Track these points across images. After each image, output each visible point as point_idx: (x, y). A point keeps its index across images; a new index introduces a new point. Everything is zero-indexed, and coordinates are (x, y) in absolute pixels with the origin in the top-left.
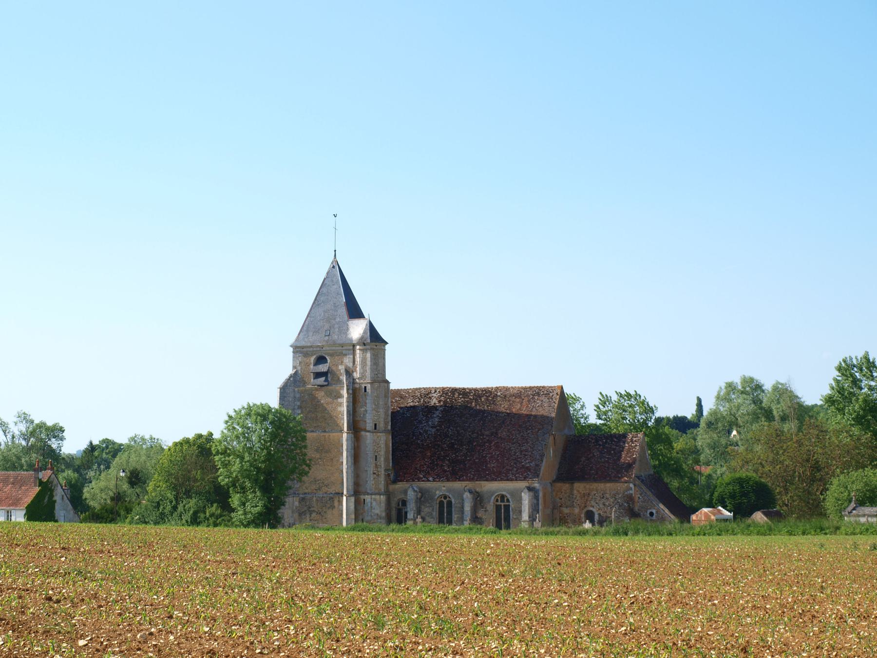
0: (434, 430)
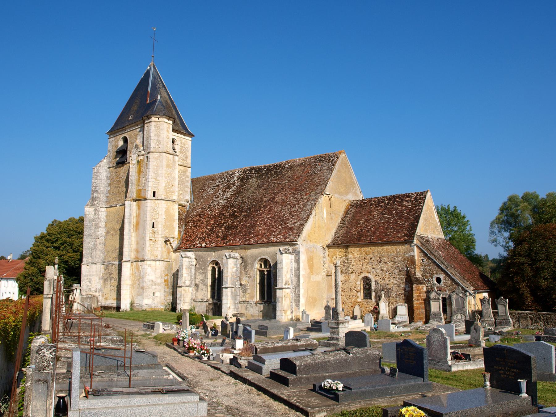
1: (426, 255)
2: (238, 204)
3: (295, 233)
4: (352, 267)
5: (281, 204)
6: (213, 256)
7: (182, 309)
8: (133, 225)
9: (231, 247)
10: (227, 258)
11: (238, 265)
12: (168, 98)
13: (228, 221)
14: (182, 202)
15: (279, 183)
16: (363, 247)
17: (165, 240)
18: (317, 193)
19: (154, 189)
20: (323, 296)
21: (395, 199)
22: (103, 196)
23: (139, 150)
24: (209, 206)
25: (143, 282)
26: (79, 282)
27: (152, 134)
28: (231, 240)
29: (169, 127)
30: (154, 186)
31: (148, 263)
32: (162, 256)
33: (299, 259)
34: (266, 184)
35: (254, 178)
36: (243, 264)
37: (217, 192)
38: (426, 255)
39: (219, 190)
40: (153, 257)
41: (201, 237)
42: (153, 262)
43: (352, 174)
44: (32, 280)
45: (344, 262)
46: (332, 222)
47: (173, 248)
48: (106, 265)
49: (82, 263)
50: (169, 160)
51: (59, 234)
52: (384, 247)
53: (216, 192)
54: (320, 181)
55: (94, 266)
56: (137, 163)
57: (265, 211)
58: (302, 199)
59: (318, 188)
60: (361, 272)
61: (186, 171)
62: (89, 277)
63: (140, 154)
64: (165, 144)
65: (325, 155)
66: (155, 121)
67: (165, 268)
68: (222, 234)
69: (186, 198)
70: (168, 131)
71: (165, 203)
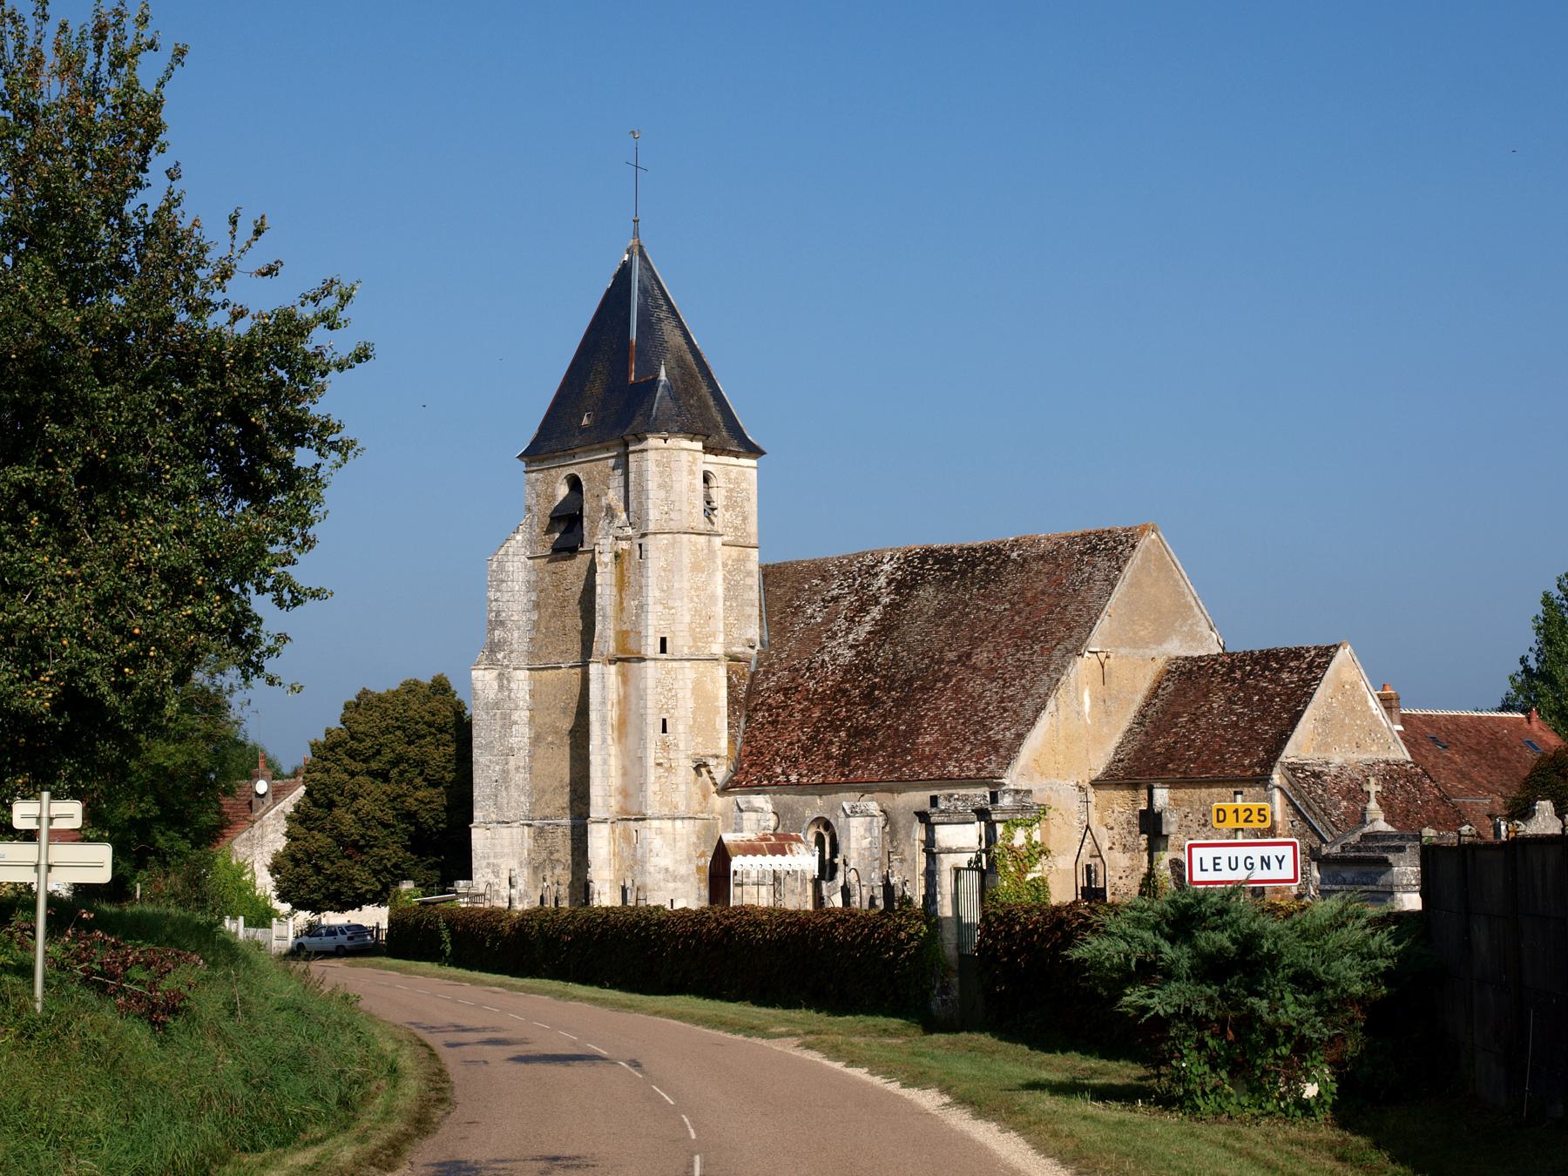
0: (849, 654)
1: (1298, 811)
2: (884, 665)
3: (1002, 757)
5: (983, 675)
6: (816, 806)
8: (612, 725)
10: (848, 816)
11: (877, 832)
12: (686, 346)
13: (855, 713)
14: (737, 649)
15: (989, 610)
18: (1068, 651)
19: (663, 632)
21: (1268, 661)
22: (518, 638)
23: (617, 523)
24: (811, 663)
25: (643, 872)
26: (467, 875)
27: (652, 486)
28: (858, 767)
30: (662, 622)
31: (655, 823)
32: (688, 806)
34: (956, 609)
35: (930, 583)
36: (887, 829)
37: (832, 621)
38: (1298, 811)
39: (837, 613)
40: (667, 809)
41: (788, 756)
42: (666, 821)
43: (1182, 583)
44: (318, 870)
46: (1108, 722)
47: (715, 784)
48: (539, 828)
51: (383, 733)
52: (1213, 790)
53: (829, 620)
54: (1080, 616)
55: (504, 831)
57: (945, 690)
58: (1033, 663)
59: (1071, 636)
62: (492, 860)
63: (620, 533)
64: (686, 508)
65: (1109, 531)
66: (657, 449)
67: (698, 838)
68: (840, 749)
69: (748, 637)
71: (692, 667)
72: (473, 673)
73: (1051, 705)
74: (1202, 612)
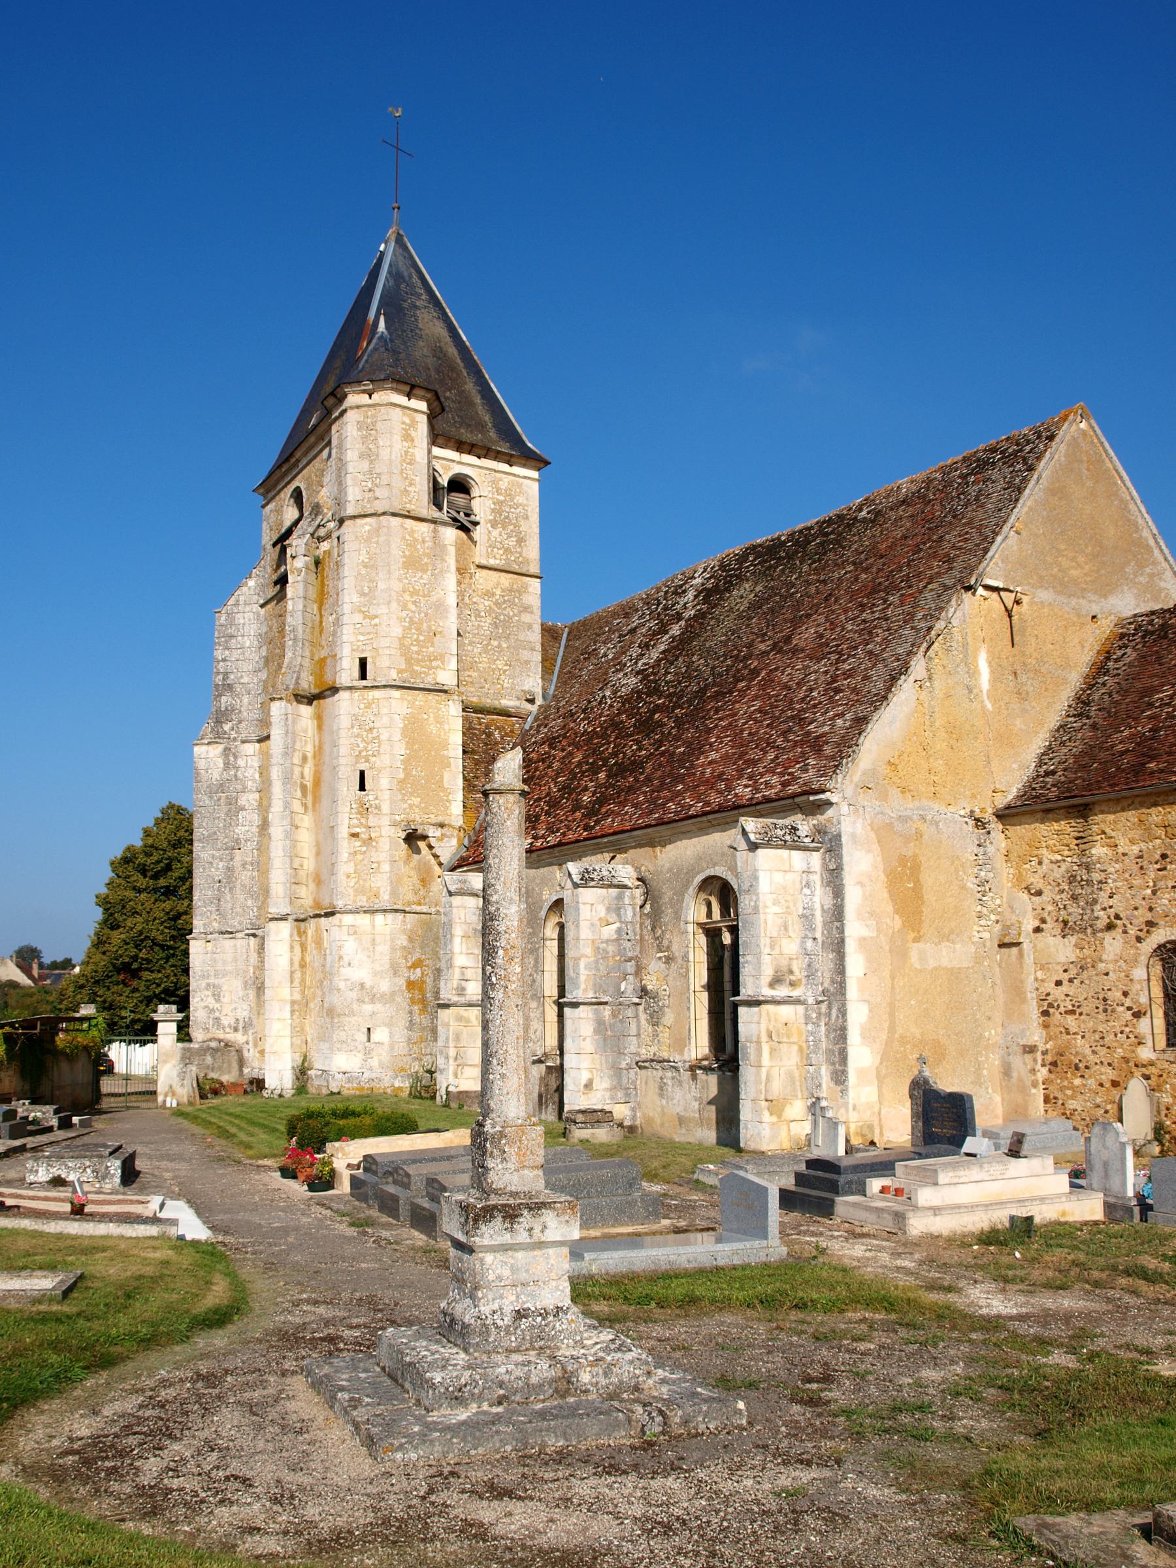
3: (827, 758)
4: (1111, 902)
7: (451, 1089)
9: (605, 840)
10: (576, 885)
11: (630, 913)
16: (1155, 805)
17: (403, 835)
18: (946, 588)
19: (363, 650)
20: (981, 1036)
24: (589, 702)
27: (351, 455)
28: (609, 813)
29: (413, 424)
30: (362, 638)
31: (348, 919)
32: (394, 893)
33: (839, 868)
36: (648, 906)
37: (624, 653)
40: (364, 899)
42: (362, 915)
43: (1132, 506)
45: (1072, 879)
46: (1024, 711)
47: (440, 864)
49: (191, 932)
50: (416, 540)
51: (174, 847)
55: (227, 943)
56: (313, 567)
57: (749, 688)
59: (951, 569)
60: (1150, 924)
61: (521, 591)
62: (212, 980)
64: (398, 483)
66: (358, 407)
67: (411, 940)
69: (526, 688)
70: (407, 437)
71: (402, 699)
72: (196, 749)
73: (918, 667)
74: (1166, 559)
